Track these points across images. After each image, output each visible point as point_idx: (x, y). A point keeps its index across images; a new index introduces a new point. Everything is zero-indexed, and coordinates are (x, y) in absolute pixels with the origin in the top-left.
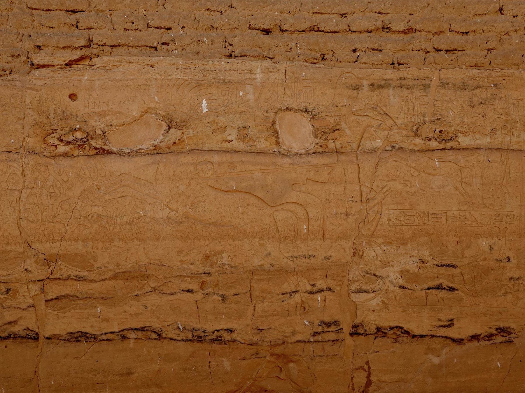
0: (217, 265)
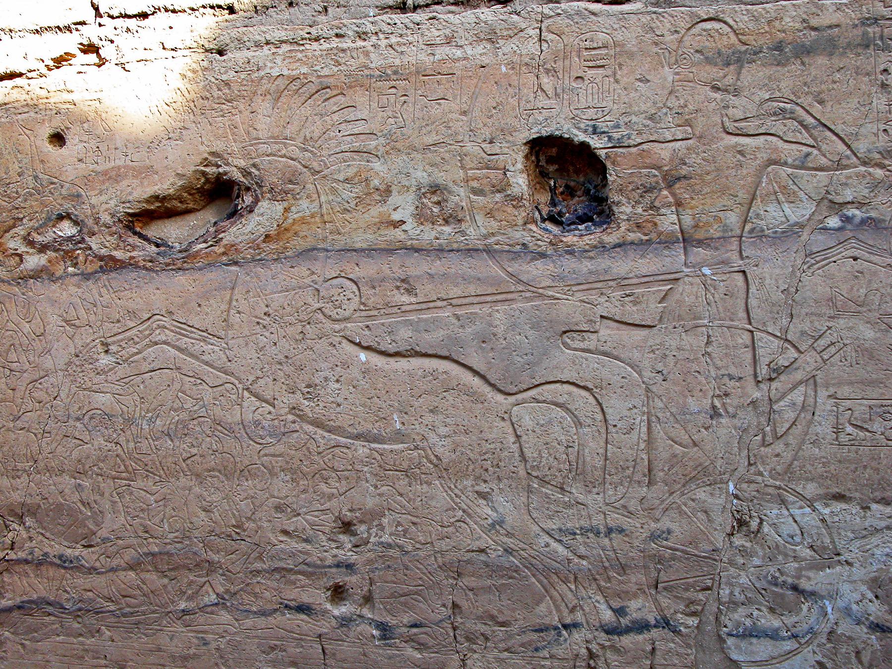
0: (370, 546)
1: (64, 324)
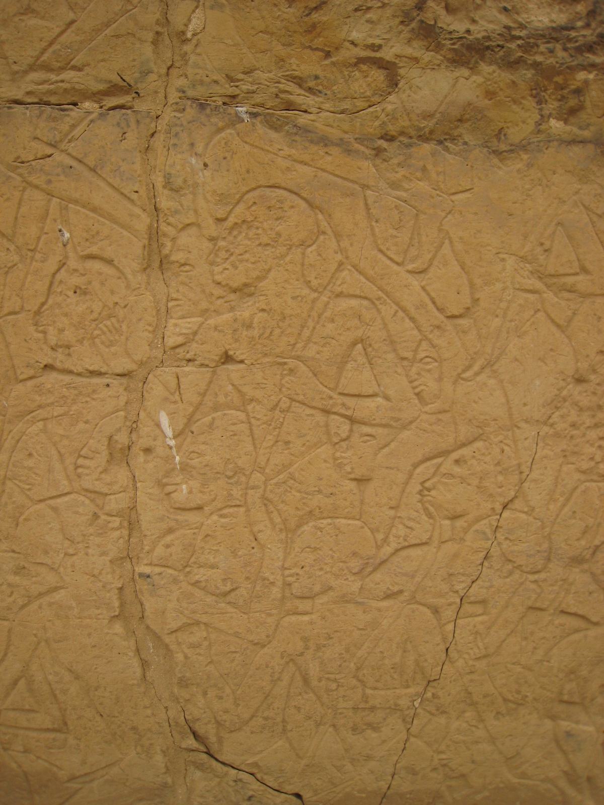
1: (539, 285)
